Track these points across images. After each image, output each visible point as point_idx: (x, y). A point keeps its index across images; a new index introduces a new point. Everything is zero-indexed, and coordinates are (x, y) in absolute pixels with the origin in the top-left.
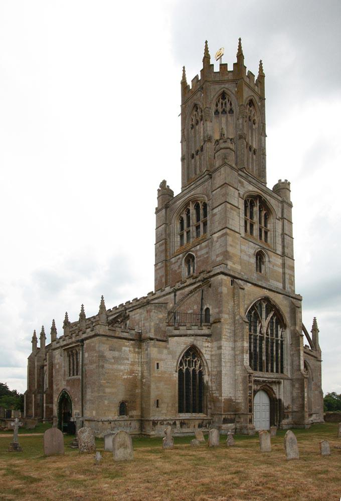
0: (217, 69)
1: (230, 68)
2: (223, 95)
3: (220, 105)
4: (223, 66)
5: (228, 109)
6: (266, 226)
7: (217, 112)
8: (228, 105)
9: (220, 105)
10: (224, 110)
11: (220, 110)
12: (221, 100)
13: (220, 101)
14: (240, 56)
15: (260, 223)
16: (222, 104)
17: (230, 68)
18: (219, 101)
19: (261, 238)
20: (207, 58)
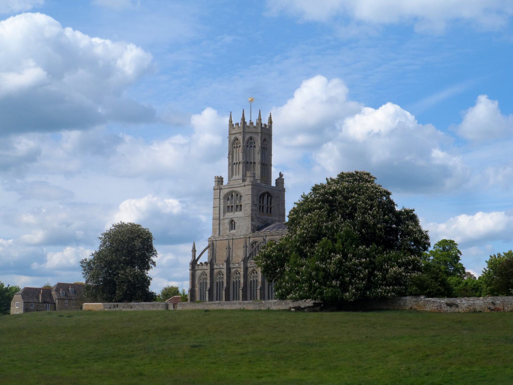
0: (248, 124)
1: (255, 124)
2: (251, 138)
3: (249, 143)
4: (252, 123)
5: (253, 146)
6: (271, 205)
7: (247, 146)
8: (253, 144)
9: (249, 143)
10: (251, 145)
11: (249, 146)
12: (250, 141)
13: (249, 141)
14: (260, 119)
15: (267, 204)
16: (250, 142)
17: (255, 124)
18: (249, 140)
19: (267, 212)
20: (243, 119)
